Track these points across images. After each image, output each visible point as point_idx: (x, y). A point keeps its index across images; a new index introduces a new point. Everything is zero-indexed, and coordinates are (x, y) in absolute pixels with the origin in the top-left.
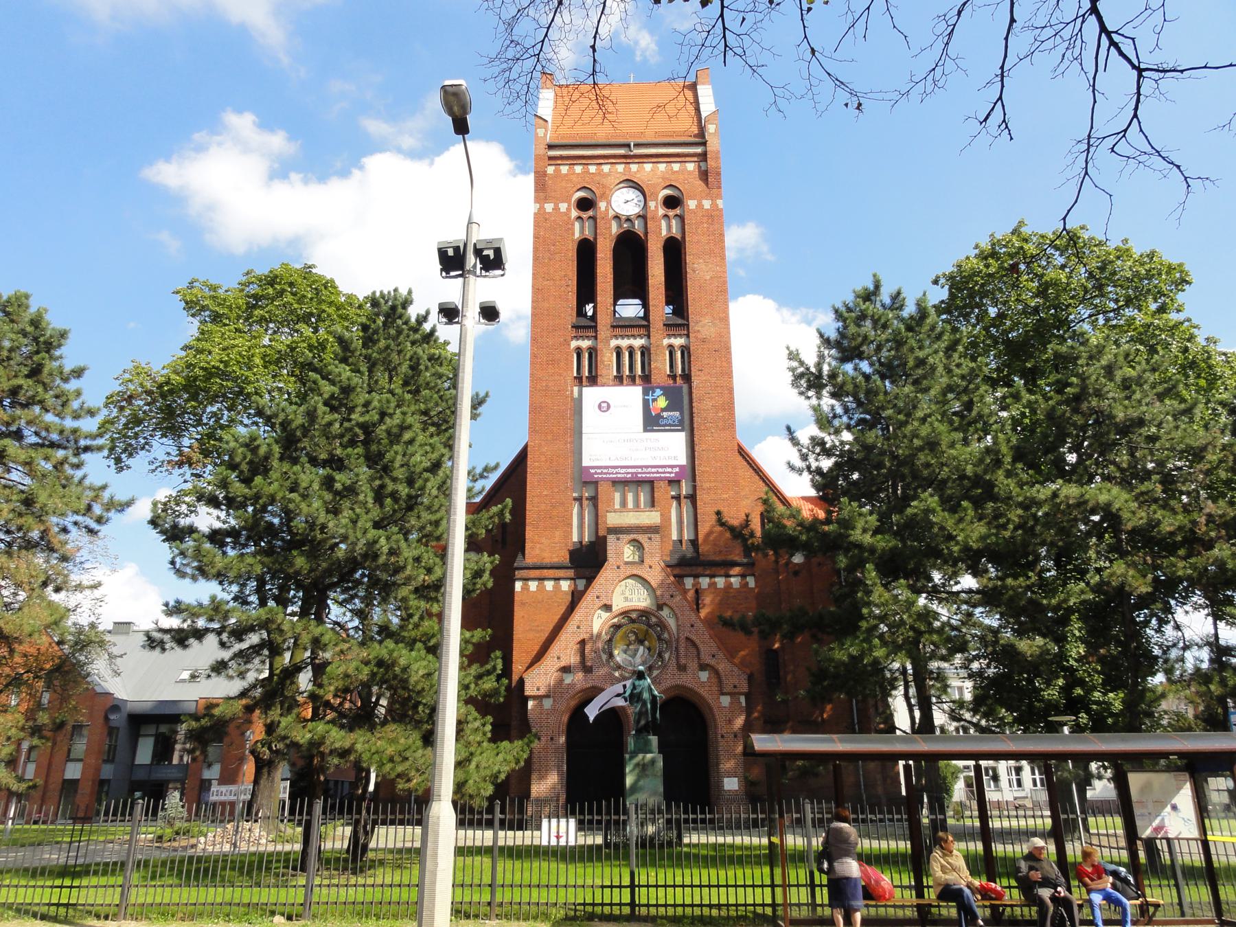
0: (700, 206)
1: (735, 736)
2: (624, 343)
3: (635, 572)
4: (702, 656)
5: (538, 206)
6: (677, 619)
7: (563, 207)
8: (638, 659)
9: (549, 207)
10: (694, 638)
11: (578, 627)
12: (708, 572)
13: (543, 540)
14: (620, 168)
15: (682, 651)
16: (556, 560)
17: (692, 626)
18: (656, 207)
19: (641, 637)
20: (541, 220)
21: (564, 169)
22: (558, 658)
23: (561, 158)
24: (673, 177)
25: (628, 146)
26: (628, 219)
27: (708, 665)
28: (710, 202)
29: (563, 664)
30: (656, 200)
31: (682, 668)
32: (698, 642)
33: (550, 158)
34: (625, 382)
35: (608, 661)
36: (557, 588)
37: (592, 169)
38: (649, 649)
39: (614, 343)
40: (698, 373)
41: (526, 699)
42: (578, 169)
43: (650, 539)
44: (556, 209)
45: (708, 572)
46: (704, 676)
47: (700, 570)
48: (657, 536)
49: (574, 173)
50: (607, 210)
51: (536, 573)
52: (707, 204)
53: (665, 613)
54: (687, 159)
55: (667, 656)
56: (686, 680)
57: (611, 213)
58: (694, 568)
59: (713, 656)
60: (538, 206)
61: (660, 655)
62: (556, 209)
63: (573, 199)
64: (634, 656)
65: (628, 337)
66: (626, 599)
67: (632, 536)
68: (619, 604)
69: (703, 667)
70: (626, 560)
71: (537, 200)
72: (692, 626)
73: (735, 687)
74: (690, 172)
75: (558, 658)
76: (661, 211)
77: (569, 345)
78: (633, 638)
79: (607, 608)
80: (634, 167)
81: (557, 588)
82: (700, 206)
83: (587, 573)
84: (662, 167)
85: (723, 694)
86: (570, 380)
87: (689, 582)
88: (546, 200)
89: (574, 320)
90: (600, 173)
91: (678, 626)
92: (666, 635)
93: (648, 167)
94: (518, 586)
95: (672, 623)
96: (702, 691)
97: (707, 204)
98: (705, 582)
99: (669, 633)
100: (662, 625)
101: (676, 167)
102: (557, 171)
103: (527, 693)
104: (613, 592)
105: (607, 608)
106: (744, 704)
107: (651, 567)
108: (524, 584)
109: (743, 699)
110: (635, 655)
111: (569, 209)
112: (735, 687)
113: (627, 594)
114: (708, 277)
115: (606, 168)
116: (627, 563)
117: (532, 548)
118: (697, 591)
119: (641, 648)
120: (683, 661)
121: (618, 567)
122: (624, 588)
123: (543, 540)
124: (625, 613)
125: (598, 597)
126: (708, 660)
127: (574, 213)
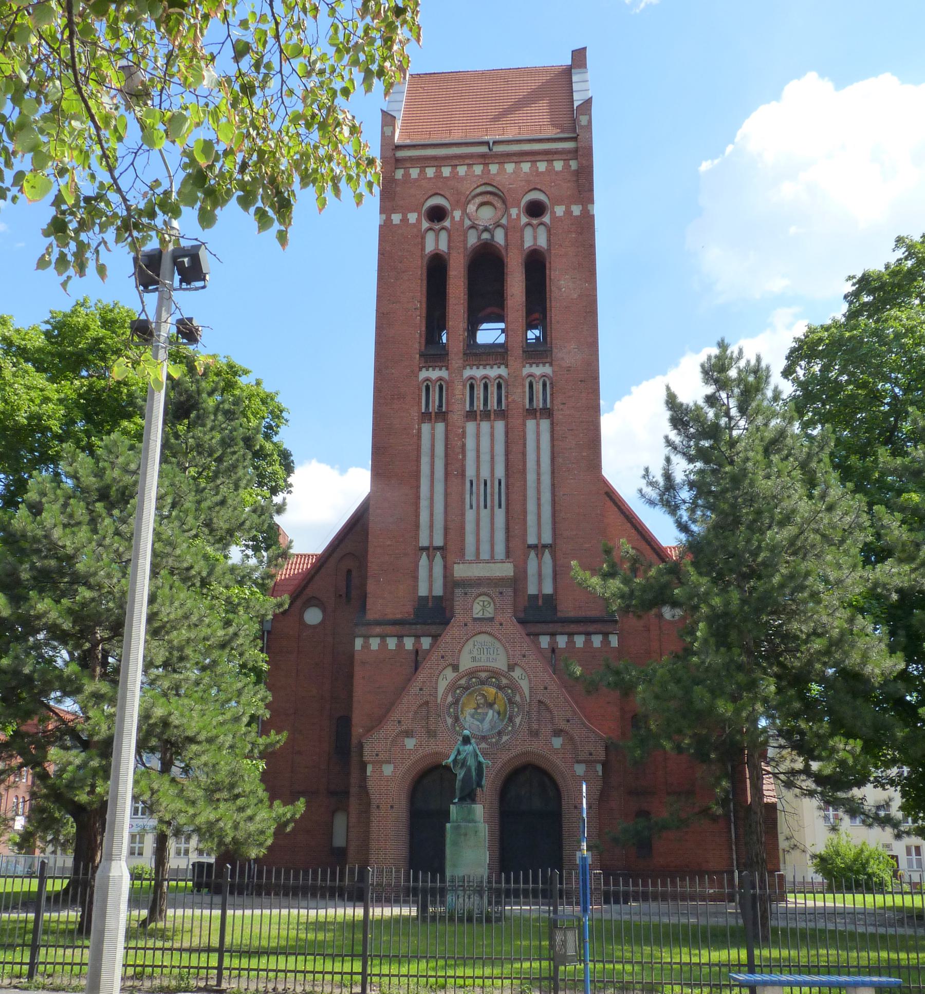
0: (568, 212)
2: (478, 373)
3: (484, 629)
6: (530, 681)
7: (412, 217)
8: (486, 725)
9: (396, 218)
10: (547, 701)
11: (421, 689)
14: (478, 169)
16: (399, 616)
17: (546, 688)
18: (518, 215)
19: (490, 699)
20: (386, 232)
21: (414, 173)
22: (399, 722)
23: (410, 159)
25: (487, 143)
27: (561, 730)
28: (580, 207)
29: (404, 727)
30: (519, 207)
31: (535, 734)
32: (551, 706)
34: (478, 417)
35: (453, 726)
36: (400, 645)
37: (446, 171)
38: (499, 713)
39: (468, 373)
40: (562, 406)
42: (430, 172)
43: (501, 593)
44: (405, 220)
45: (567, 630)
46: (557, 742)
47: (558, 627)
48: (510, 590)
49: (426, 178)
50: (462, 220)
51: (378, 630)
52: (576, 210)
53: (517, 673)
54: (556, 157)
55: (518, 720)
56: (535, 746)
57: (467, 223)
58: (551, 625)
59: (568, 721)
60: (384, 216)
61: (511, 719)
62: (405, 220)
63: (425, 208)
64: (482, 721)
65: (485, 366)
66: (474, 659)
67: (482, 590)
68: (466, 663)
69: (558, 733)
70: (475, 616)
71: (383, 210)
72: (546, 688)
73: (591, 754)
74: (557, 173)
75: (399, 722)
76: (524, 219)
77: (417, 376)
78: (482, 701)
79: (455, 668)
81: (400, 645)
82: (568, 212)
83: (433, 629)
84: (526, 167)
85: (578, 762)
86: (415, 414)
87: (545, 641)
88: (394, 211)
89: (423, 348)
90: (454, 175)
91: (531, 688)
92: (518, 698)
93: (510, 167)
94: (358, 643)
95: (524, 685)
97: (576, 210)
98: (562, 641)
99: (521, 697)
100: (514, 687)
101: (542, 166)
102: (407, 175)
103: (365, 759)
104: (460, 651)
105: (455, 668)
106: (600, 773)
107: (501, 624)
108: (365, 642)
109: (599, 768)
110: (484, 719)
111: (419, 220)
113: (475, 653)
114: (575, 296)
115: (462, 170)
116: (475, 619)
118: (553, 651)
119: (491, 712)
121: (466, 625)
122: (471, 646)
124: (472, 673)
125: (443, 657)
126: (563, 725)
127: (425, 224)
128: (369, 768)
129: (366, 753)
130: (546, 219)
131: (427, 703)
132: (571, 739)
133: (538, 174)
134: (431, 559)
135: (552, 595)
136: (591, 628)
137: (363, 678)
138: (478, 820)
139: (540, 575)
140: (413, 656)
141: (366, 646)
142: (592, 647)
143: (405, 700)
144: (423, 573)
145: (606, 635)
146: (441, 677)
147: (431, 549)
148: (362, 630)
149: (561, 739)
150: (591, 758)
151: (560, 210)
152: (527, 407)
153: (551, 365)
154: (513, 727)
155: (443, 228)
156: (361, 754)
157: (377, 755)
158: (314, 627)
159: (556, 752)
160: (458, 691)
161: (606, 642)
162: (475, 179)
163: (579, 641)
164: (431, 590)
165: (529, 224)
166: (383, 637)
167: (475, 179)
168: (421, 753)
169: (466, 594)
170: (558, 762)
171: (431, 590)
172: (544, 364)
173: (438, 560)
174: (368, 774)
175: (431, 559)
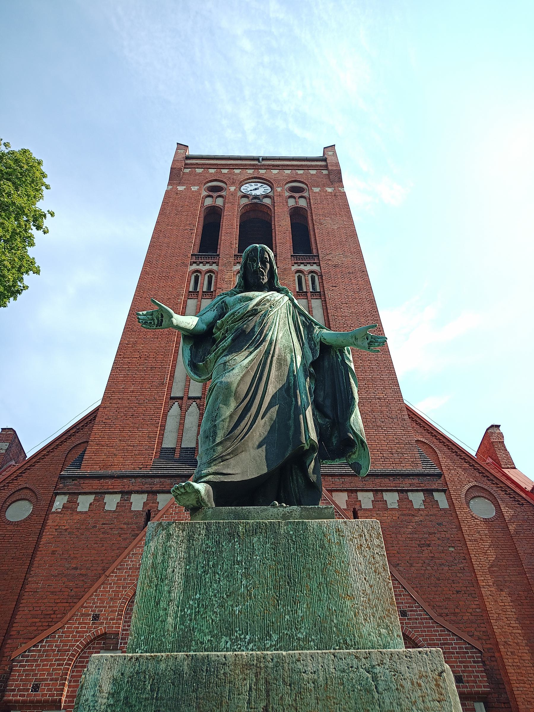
5: (170, 187)
7: (195, 188)
14: (250, 171)
22: (96, 617)
24: (297, 177)
26: (256, 197)
29: (101, 630)
33: (186, 164)
57: (240, 194)
75: (96, 617)
80: (262, 171)
88: (180, 184)
130: (306, 194)
133: (297, 174)
134: (183, 411)
136: (405, 484)
137: (53, 552)
144: (172, 423)
147: (185, 399)
148: (71, 486)
151: (316, 190)
152: (298, 290)
153: (319, 265)
155: (220, 196)
157: (36, 688)
162: (247, 175)
164: (180, 439)
165: (291, 197)
167: (247, 175)
171: (180, 439)
172: (312, 264)
173: (193, 408)
175: (183, 411)
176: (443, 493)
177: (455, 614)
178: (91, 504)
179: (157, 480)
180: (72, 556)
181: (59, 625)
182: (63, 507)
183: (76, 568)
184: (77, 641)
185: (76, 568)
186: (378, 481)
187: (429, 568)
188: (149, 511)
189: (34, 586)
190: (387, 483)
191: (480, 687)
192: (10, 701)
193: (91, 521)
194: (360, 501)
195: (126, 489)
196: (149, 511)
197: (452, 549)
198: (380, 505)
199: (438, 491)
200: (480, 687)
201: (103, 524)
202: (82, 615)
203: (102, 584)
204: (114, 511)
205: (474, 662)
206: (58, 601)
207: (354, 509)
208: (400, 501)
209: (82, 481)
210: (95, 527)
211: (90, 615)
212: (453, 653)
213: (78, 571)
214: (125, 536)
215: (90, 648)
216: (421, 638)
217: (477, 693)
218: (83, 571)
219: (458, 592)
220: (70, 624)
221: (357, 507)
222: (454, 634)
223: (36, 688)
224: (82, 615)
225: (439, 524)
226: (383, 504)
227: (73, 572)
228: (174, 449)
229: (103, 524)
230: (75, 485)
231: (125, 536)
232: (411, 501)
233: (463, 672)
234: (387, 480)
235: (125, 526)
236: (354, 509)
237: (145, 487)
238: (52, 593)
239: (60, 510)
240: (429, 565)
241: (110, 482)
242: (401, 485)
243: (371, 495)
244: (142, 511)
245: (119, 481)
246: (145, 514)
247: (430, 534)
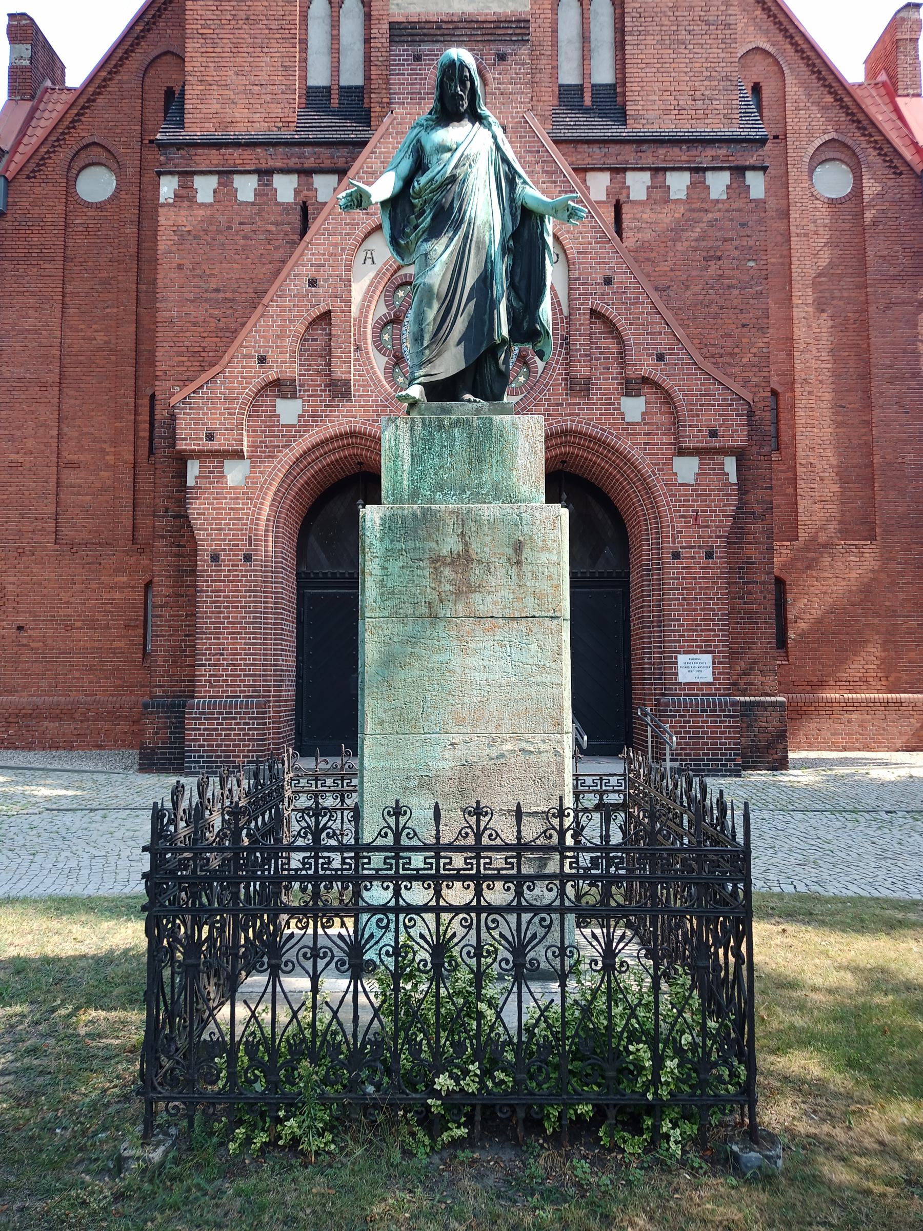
1: (709, 555)
4: (633, 356)
10: (611, 312)
11: (313, 283)
12: (648, 160)
13: (230, 76)
15: (580, 342)
17: (608, 281)
22: (262, 360)
27: (645, 380)
29: (272, 375)
32: (621, 323)
36: (265, 193)
41: (181, 460)
45: (649, 161)
47: (629, 155)
51: (214, 157)
59: (660, 357)
73: (713, 434)
75: (262, 360)
81: (265, 193)
85: (682, 452)
94: (168, 187)
96: (625, 444)
106: (733, 479)
109: (730, 465)
112: (713, 434)
117: (202, 98)
118: (618, 208)
120: (581, 370)
123: (230, 76)
126: (647, 367)
128: (193, 469)
129: (181, 433)
131: (326, 316)
132: (668, 398)
135: (613, 87)
136: (705, 156)
137: (180, 267)
138: (524, 489)
139: (585, 38)
140: (296, 219)
141: (185, 195)
142: (706, 199)
143: (273, 309)
145: (739, 171)
146: (361, 255)
149: (642, 399)
150: (715, 443)
154: (528, 376)
156: (172, 438)
157: (210, 437)
158: (99, 206)
159: (629, 428)
160: (401, 294)
161: (738, 188)
163: (678, 183)
166: (225, 174)
168: (313, 436)
169: (418, 58)
170: (636, 454)
171: (336, 70)
174: (191, 482)
176: (760, 174)
177: (732, 355)
178: (215, 191)
179: (308, 150)
180: (208, 272)
181: (217, 369)
182: (176, 196)
183: (217, 290)
184: (245, 388)
185: (217, 290)
186: (662, 151)
187: (711, 291)
188: (304, 203)
189: (166, 314)
190: (679, 155)
191: (736, 441)
192: (185, 450)
193: (222, 219)
194: (628, 187)
195: (263, 166)
196: (304, 203)
197: (751, 264)
198: (658, 194)
199: (753, 168)
200: (736, 441)
201: (241, 224)
202: (244, 356)
203: (261, 317)
204: (253, 204)
205: (737, 415)
206: (205, 335)
207: (618, 201)
208: (692, 186)
209: (192, 152)
210: (229, 228)
211: (253, 357)
212: (714, 405)
213: (222, 295)
214: (277, 243)
215: (262, 396)
216: (676, 388)
217: (733, 447)
218: (229, 295)
219: (743, 326)
220: (231, 367)
221: (623, 198)
222: (720, 383)
223: (210, 437)
224: (244, 356)
225: (743, 225)
226: (664, 192)
227: (214, 295)
228: (328, 89)
229: (241, 224)
230: (183, 157)
231: (277, 243)
232: (708, 187)
233: (720, 426)
234: (676, 150)
235: (273, 228)
236: (618, 201)
237: (293, 162)
238: (195, 324)
239: (171, 201)
240: (712, 287)
241: (236, 153)
242: (698, 159)
243: (646, 176)
244: (295, 204)
245: (249, 151)
246: (299, 208)
247: (726, 240)
